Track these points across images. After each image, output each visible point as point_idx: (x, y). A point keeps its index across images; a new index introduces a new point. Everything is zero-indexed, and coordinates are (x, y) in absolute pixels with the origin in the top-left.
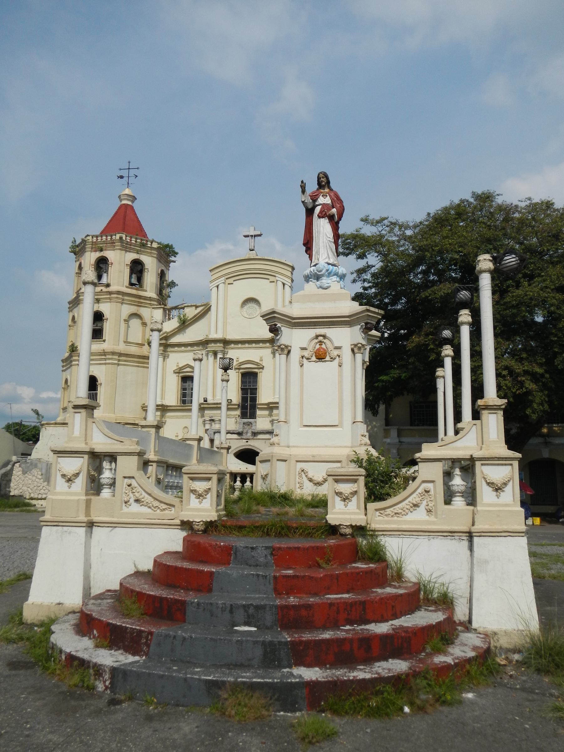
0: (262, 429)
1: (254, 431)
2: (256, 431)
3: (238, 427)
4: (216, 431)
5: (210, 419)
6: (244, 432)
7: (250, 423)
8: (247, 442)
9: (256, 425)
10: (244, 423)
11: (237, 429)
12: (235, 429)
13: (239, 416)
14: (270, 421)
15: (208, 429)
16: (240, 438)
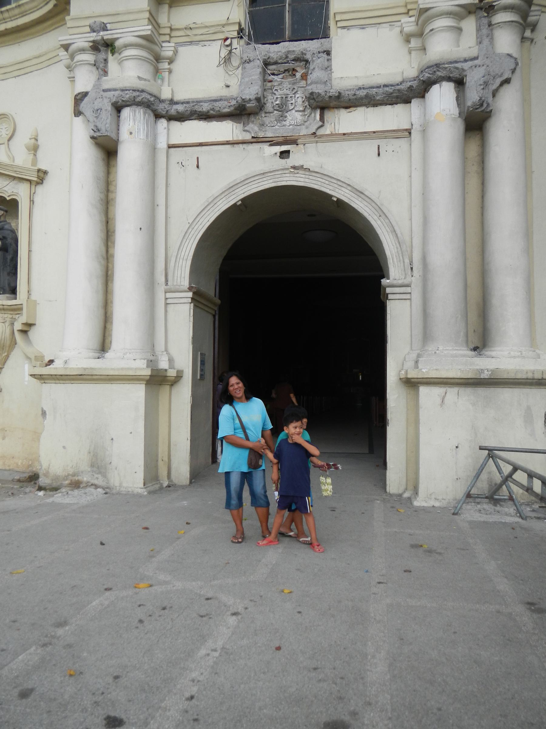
0: (360, 83)
1: (319, 89)
2: (333, 92)
3: (234, 82)
4: (127, 96)
5: (93, 36)
6: (269, 107)
7: (296, 60)
8: (285, 154)
9: (328, 68)
10: (266, 64)
11: (234, 91)
12: (225, 93)
13: (241, 30)
14: (408, 37)
15: (86, 94)
16: (248, 137)
